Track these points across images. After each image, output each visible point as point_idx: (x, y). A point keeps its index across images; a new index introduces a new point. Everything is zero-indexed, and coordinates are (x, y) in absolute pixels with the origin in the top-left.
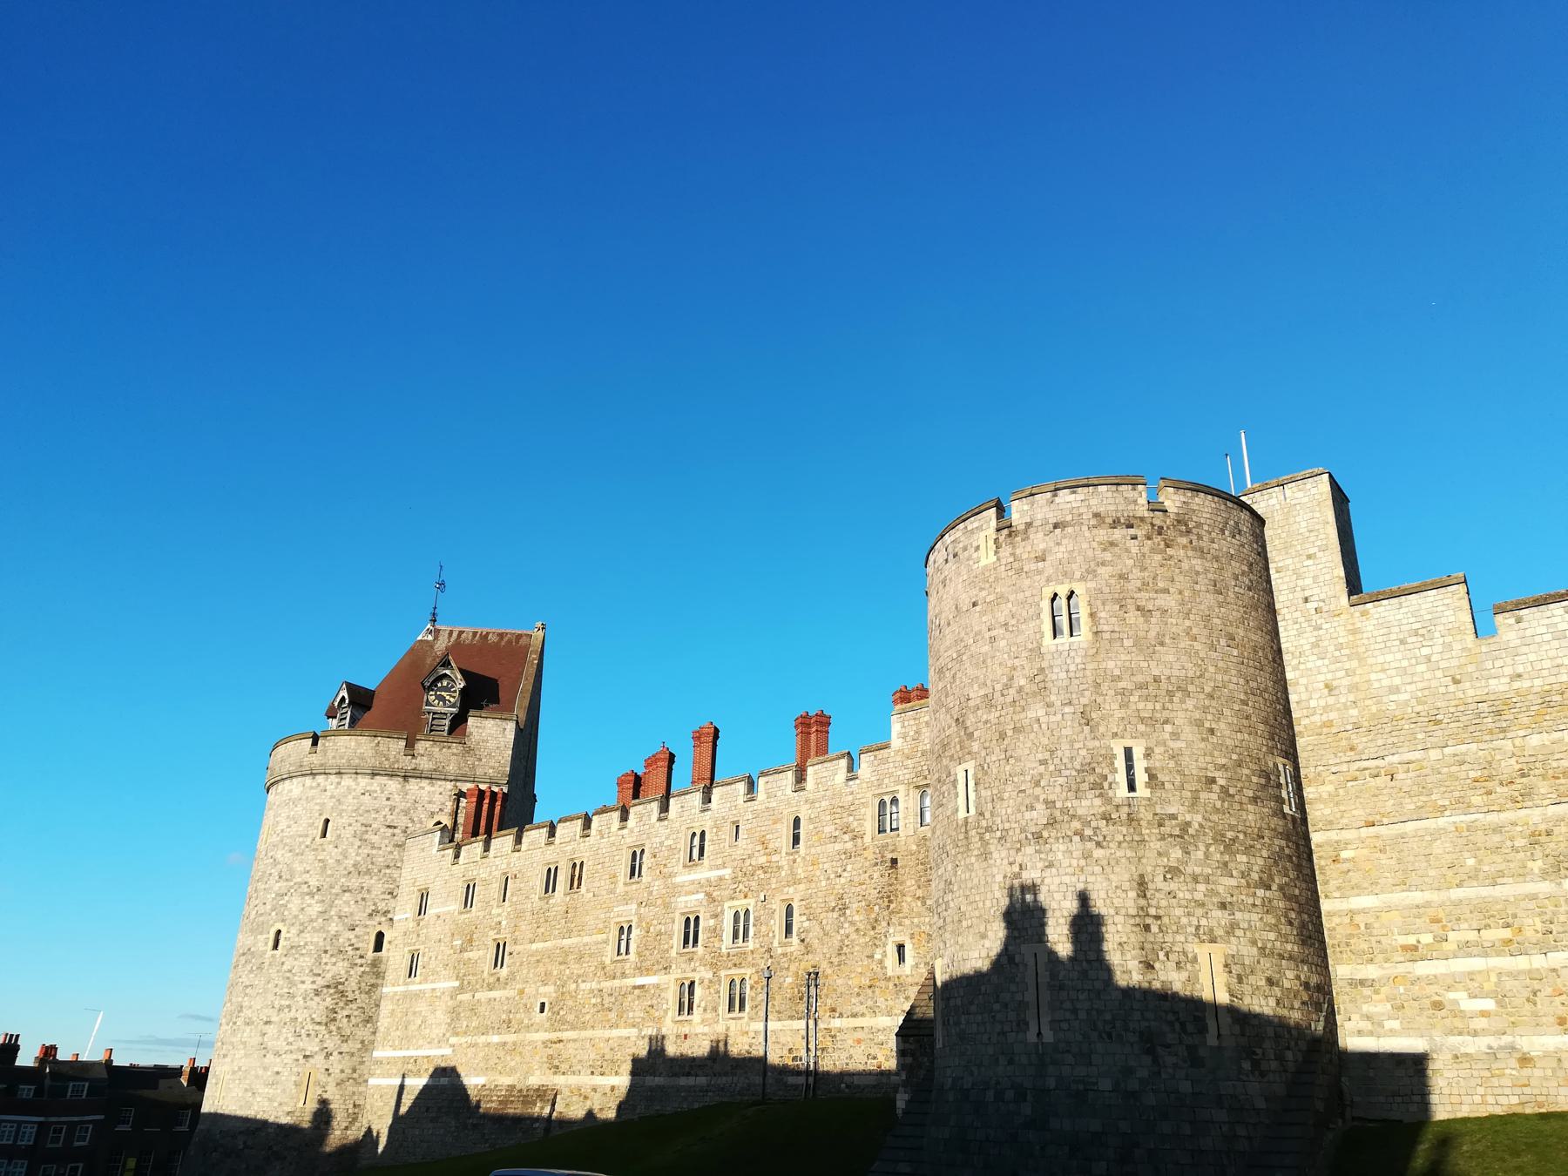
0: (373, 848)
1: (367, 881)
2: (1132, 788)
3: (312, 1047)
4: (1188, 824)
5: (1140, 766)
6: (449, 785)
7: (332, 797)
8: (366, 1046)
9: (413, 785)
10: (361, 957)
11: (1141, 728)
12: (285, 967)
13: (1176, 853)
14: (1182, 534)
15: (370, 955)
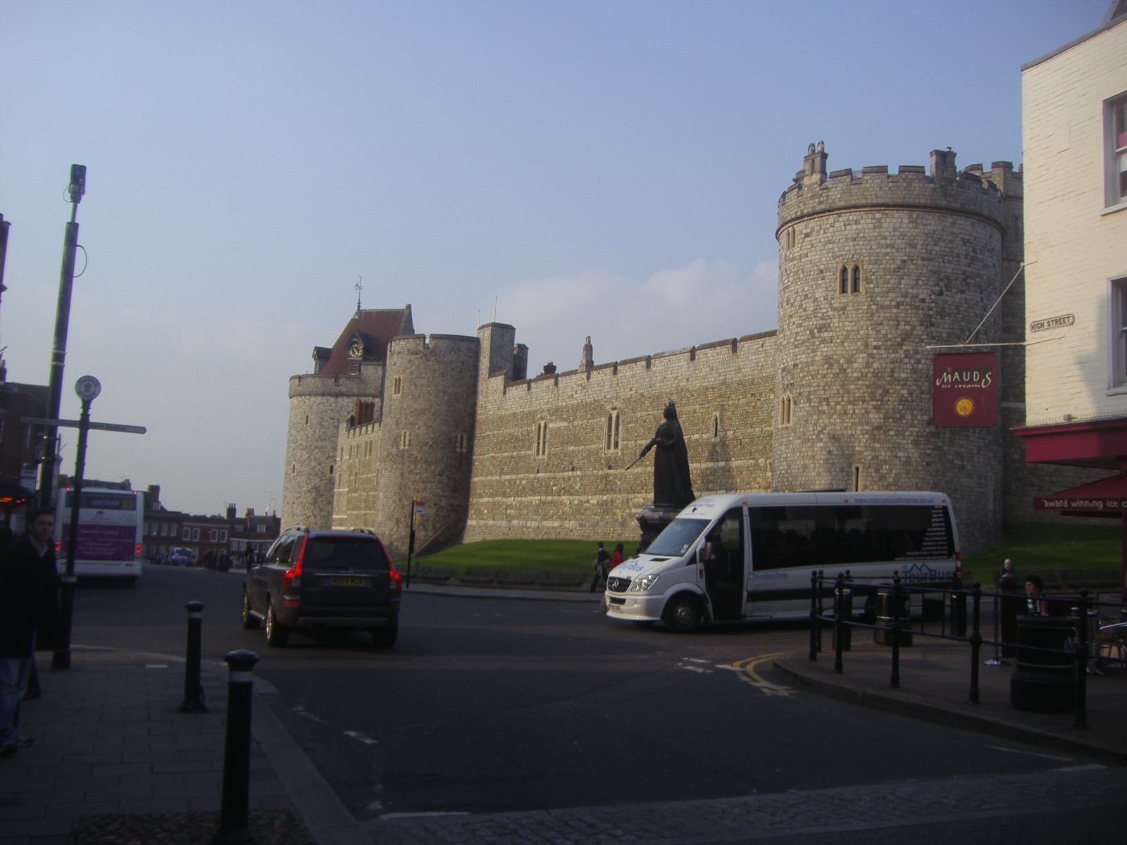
0: (326, 428)
1: (324, 443)
2: (404, 446)
3: (309, 513)
4: (417, 457)
5: (407, 439)
6: (355, 398)
7: (308, 406)
8: (330, 514)
9: (340, 400)
10: (325, 476)
11: (410, 426)
12: (298, 480)
13: (413, 466)
14: (433, 356)
15: (328, 475)
